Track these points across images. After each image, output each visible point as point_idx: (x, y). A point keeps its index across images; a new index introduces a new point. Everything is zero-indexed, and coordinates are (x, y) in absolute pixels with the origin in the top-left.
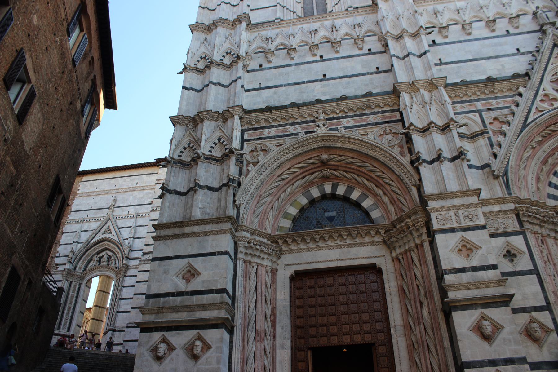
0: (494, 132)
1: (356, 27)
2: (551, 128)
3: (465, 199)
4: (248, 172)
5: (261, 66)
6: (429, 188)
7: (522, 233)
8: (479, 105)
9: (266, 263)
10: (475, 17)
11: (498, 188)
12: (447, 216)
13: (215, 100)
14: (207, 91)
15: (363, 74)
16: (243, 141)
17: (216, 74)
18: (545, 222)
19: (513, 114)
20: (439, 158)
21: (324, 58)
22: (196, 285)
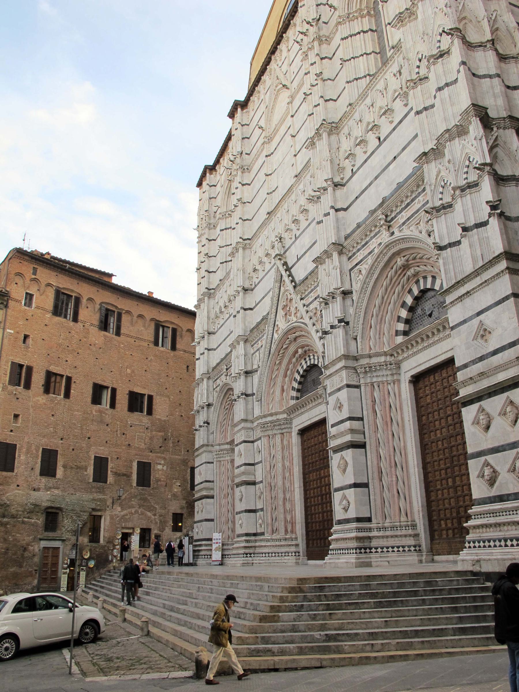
9: (226, 459)
18: (274, 426)
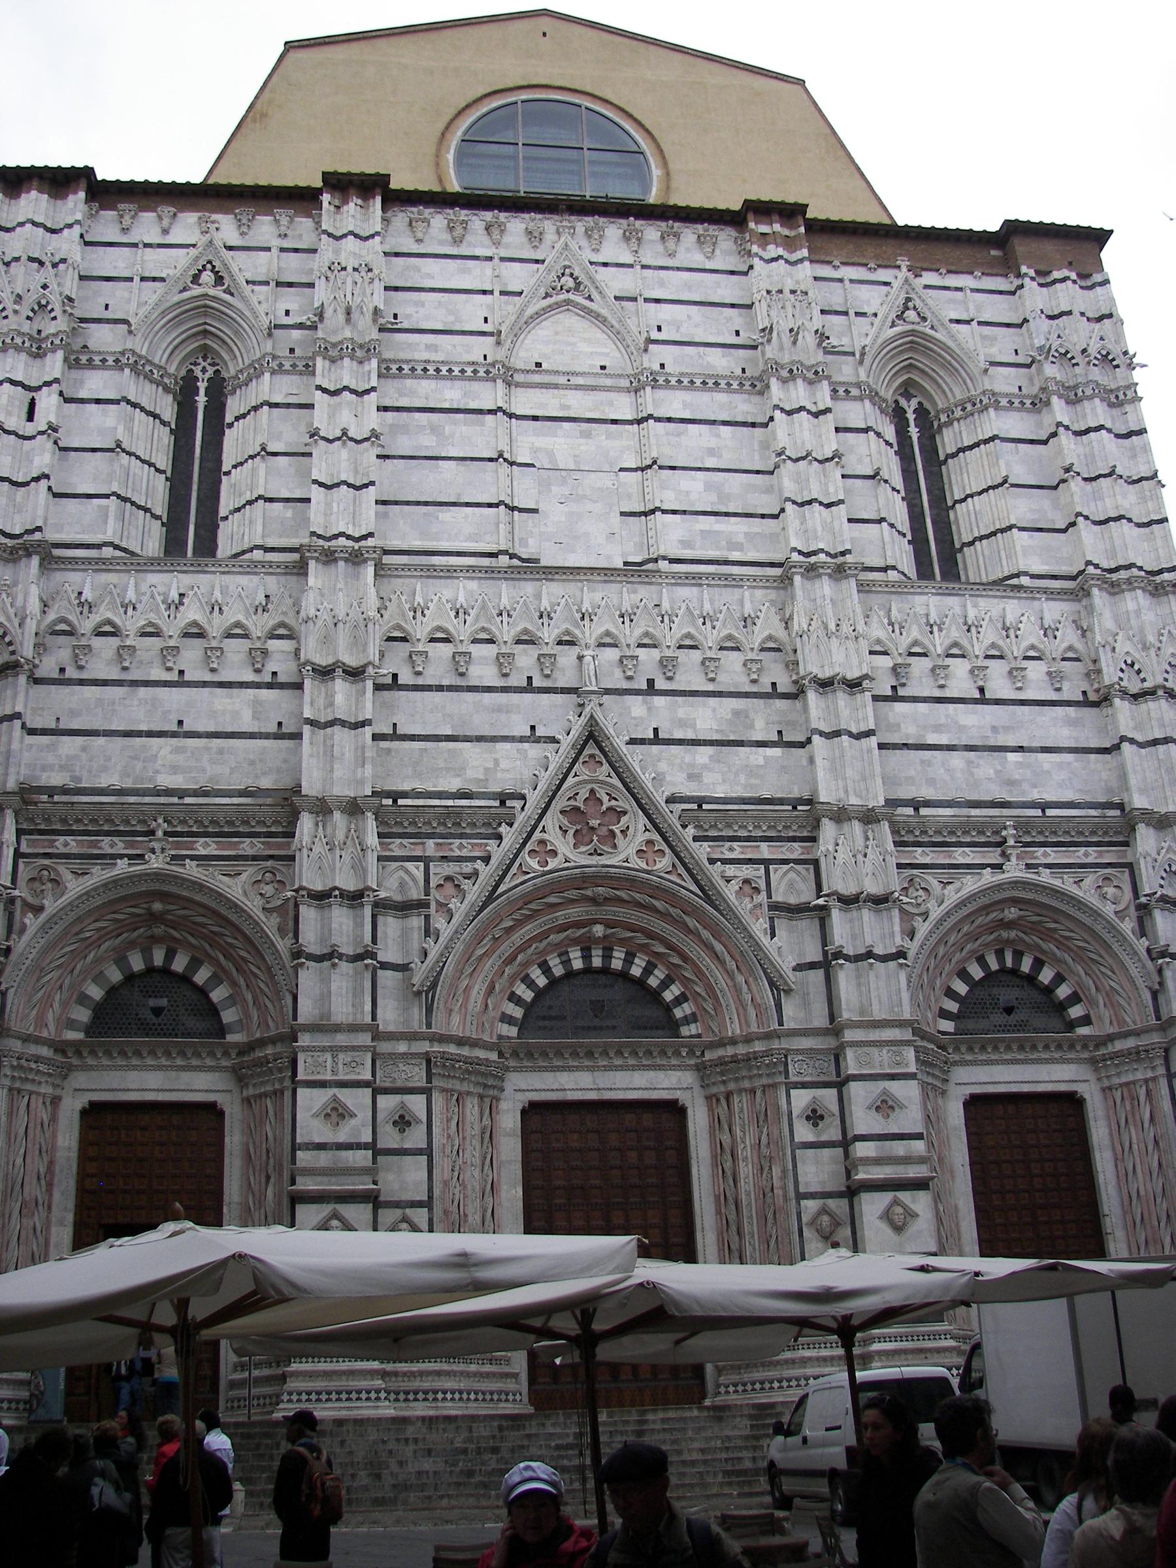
0: (440, 905)
1: (260, 610)
2: (533, 906)
3: (352, 1035)
4: (23, 929)
5: (62, 670)
6: (307, 1010)
7: (427, 1091)
8: (430, 847)
9: (46, 1089)
10: (483, 629)
11: (416, 1010)
12: (321, 1060)
15: (252, 736)
16: (18, 854)
18: (470, 1073)
19: (476, 873)
20: (331, 956)
21: (187, 677)
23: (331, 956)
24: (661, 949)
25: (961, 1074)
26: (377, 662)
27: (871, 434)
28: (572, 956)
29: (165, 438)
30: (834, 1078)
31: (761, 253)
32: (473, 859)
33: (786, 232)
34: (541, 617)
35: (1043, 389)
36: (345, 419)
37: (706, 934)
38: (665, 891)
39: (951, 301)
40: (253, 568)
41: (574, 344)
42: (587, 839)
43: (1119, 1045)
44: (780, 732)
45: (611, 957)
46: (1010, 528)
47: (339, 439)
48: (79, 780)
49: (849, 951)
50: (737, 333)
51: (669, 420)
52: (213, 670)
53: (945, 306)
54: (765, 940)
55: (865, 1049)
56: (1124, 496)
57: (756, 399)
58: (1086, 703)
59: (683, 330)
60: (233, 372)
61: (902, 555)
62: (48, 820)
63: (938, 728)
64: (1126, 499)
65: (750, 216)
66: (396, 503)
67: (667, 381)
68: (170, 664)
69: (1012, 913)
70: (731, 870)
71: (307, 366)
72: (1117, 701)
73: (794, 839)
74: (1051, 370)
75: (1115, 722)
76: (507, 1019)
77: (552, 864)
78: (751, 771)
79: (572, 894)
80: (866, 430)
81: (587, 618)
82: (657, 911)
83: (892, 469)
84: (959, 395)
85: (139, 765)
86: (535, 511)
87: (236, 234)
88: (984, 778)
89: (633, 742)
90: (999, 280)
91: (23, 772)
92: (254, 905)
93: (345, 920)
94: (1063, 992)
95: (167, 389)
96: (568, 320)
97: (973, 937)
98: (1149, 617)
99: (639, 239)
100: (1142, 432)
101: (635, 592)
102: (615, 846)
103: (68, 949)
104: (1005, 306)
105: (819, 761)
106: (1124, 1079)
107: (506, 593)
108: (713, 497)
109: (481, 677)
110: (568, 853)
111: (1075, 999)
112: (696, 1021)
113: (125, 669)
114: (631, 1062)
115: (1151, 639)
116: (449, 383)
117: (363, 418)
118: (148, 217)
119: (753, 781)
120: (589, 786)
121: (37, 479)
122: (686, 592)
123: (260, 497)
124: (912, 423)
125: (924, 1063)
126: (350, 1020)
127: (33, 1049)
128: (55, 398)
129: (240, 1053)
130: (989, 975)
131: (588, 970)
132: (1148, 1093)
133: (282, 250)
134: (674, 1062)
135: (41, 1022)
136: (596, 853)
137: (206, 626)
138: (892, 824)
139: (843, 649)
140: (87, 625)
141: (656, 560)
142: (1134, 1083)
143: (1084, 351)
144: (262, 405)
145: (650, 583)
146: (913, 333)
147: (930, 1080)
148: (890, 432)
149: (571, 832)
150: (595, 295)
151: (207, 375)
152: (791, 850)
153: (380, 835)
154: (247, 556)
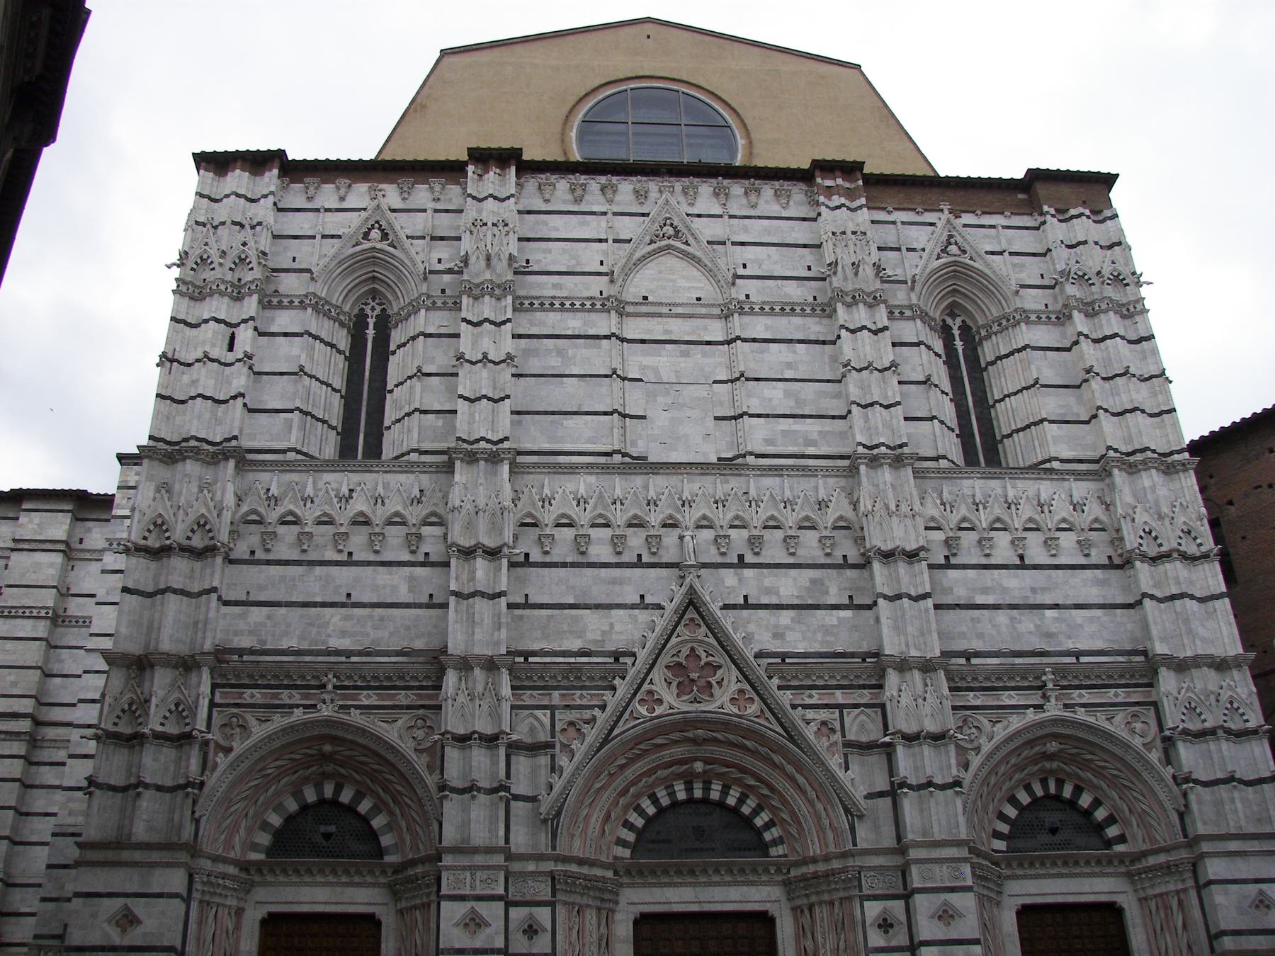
2: (642, 746)
3: (488, 857)
4: (215, 765)
5: (253, 553)
6: (450, 835)
7: (551, 904)
9: (232, 902)
10: (600, 516)
11: (543, 835)
13: (173, 628)
14: (163, 604)
16: (212, 704)
17: (179, 571)
18: (589, 889)
19: (594, 719)
20: (471, 789)
21: (355, 558)
22: (135, 937)
23: (471, 789)
24: (752, 782)
25: (1013, 887)
26: (511, 543)
27: (923, 347)
28: (676, 788)
29: (340, 363)
30: (901, 891)
31: (827, 202)
32: (592, 707)
33: (847, 185)
34: (648, 504)
35: (1066, 306)
36: (486, 345)
37: (790, 769)
38: (755, 732)
39: (986, 236)
40: (410, 468)
41: (674, 281)
42: (688, 690)
43: (1152, 861)
44: (850, 597)
45: (709, 789)
46: (1041, 421)
47: (480, 361)
48: (265, 642)
49: (912, 781)
50: (809, 268)
51: (754, 340)
52: (376, 552)
53: (982, 241)
54: (840, 773)
55: (928, 866)
56: (1138, 391)
57: (825, 321)
58: (1111, 566)
59: (764, 267)
60: (396, 310)
61: (951, 447)
62: (238, 676)
63: (985, 591)
64: (1139, 394)
65: (817, 173)
66: (528, 413)
67: (752, 309)
68: (341, 547)
69: (1053, 747)
70: (810, 714)
71: (455, 303)
72: (1138, 564)
73: (864, 687)
74: (1071, 290)
75: (1137, 582)
76: (622, 843)
77: (659, 710)
78: (827, 630)
79: (676, 736)
80: (917, 344)
81: (687, 505)
82: (748, 750)
83: (941, 375)
84: (995, 312)
85: (314, 630)
86: (643, 417)
87: (399, 199)
88: (1026, 632)
89: (726, 607)
90: (1026, 218)
91: (218, 636)
92: (407, 747)
93: (483, 759)
94: (1100, 814)
95: (342, 325)
96: (670, 261)
97: (1020, 768)
98: (1162, 492)
99: (726, 195)
100: (1151, 337)
101: (727, 482)
102: (712, 695)
103: (252, 784)
104: (1032, 239)
105: (883, 620)
106: (1157, 891)
107: (619, 486)
108: (792, 403)
109: (598, 555)
110: (672, 702)
111: (1111, 820)
112: (782, 843)
113: (304, 551)
114: (728, 878)
115: (1165, 510)
116: (571, 314)
117: (501, 344)
118: (329, 187)
119: (829, 638)
120: (690, 645)
121: (234, 398)
122: (769, 482)
123: (416, 410)
124: (957, 338)
125: (980, 877)
126: (487, 843)
127: (221, 868)
128: (250, 332)
129: (395, 872)
130: (1035, 800)
131: (690, 801)
132: (1180, 903)
133: (436, 211)
134: (764, 878)
135: (228, 844)
136: (696, 701)
137: (371, 516)
138: (947, 672)
139: (902, 525)
140: (273, 516)
141: (744, 456)
142: (1166, 894)
143: (1099, 273)
144: (418, 335)
145: (740, 475)
146: (955, 263)
147: (985, 892)
148: (938, 346)
149: (674, 684)
150: (691, 241)
151: (376, 313)
152: (862, 696)
153: (513, 688)
154: (405, 458)
